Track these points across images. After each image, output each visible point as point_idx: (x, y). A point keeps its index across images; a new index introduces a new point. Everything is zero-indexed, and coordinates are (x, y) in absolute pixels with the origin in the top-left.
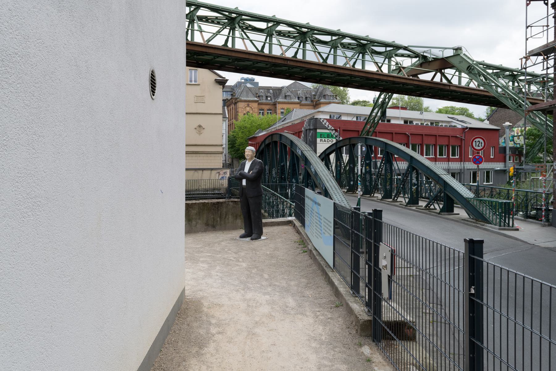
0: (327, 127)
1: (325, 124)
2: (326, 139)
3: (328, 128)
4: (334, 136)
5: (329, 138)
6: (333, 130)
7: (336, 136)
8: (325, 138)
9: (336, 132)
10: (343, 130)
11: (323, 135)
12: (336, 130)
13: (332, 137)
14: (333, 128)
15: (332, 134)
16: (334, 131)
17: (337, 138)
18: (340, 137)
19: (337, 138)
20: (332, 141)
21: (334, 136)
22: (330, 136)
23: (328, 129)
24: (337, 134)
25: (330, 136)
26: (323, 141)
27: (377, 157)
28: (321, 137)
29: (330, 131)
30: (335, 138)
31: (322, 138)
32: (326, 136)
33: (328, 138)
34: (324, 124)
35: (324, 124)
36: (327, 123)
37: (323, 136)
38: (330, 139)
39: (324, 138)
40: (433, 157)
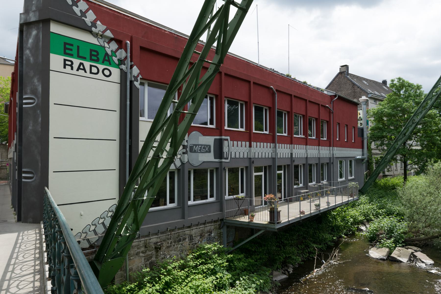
0: (90, 24)
1: (84, 14)
2: (87, 64)
3: (93, 29)
4: (115, 59)
5: (97, 61)
6: (111, 40)
7: (121, 62)
8: (84, 58)
9: (120, 47)
10: (142, 48)
11: (75, 49)
12: (121, 44)
13: (107, 59)
14: (109, 34)
15: (109, 53)
16: (114, 46)
17: (123, 67)
18: (132, 67)
19: (123, 67)
20: (106, 72)
21: (115, 59)
22: (101, 57)
23: (91, 32)
24: (122, 54)
25: (101, 57)
26: (76, 66)
27: (223, 131)
28: (65, 54)
29: (101, 41)
30: (118, 66)
31: (71, 55)
32: (85, 52)
33: (91, 60)
34: (79, 14)
35: (79, 14)
36: (90, 17)
37: (75, 52)
38: (101, 67)
39: (79, 57)
40: (304, 136)
